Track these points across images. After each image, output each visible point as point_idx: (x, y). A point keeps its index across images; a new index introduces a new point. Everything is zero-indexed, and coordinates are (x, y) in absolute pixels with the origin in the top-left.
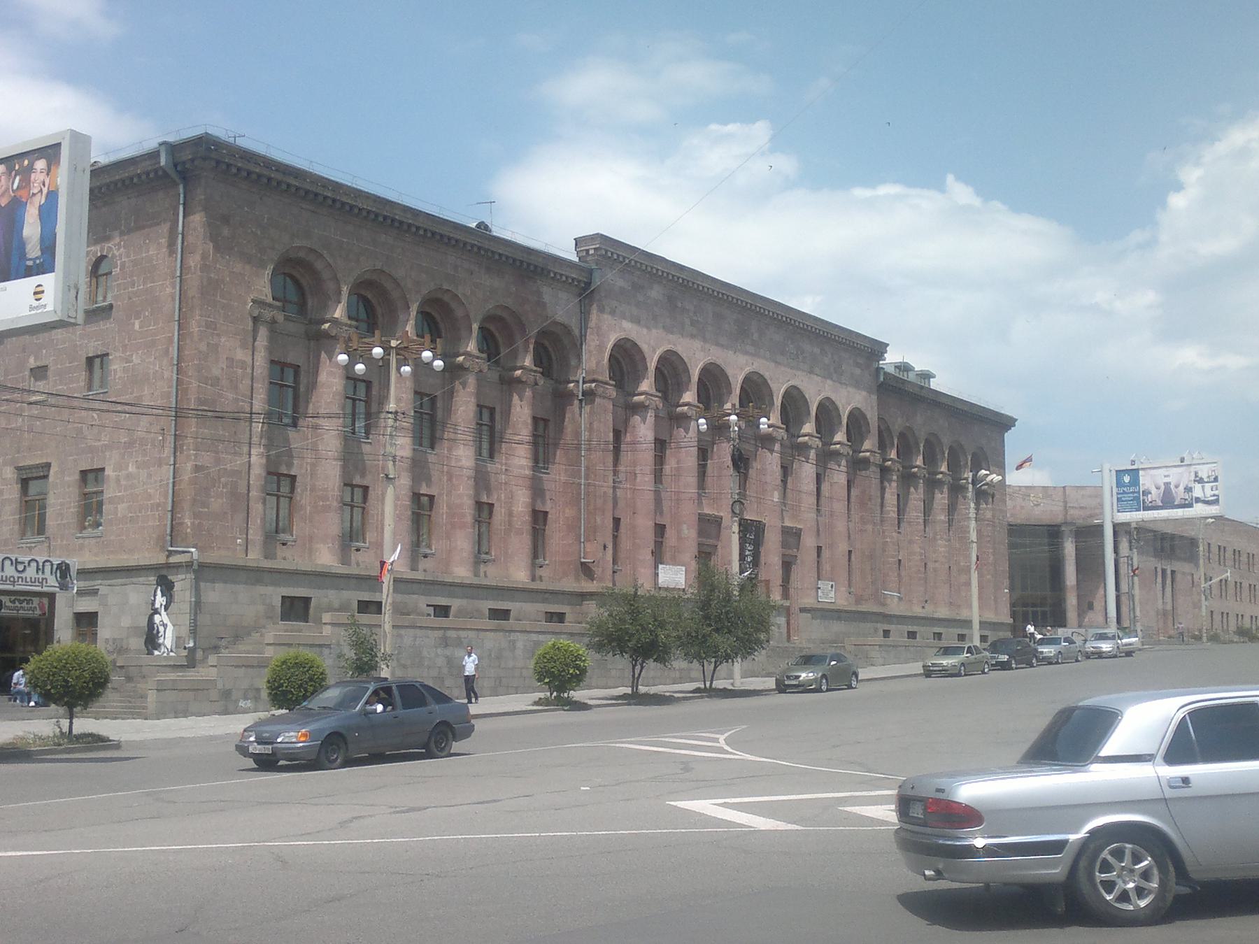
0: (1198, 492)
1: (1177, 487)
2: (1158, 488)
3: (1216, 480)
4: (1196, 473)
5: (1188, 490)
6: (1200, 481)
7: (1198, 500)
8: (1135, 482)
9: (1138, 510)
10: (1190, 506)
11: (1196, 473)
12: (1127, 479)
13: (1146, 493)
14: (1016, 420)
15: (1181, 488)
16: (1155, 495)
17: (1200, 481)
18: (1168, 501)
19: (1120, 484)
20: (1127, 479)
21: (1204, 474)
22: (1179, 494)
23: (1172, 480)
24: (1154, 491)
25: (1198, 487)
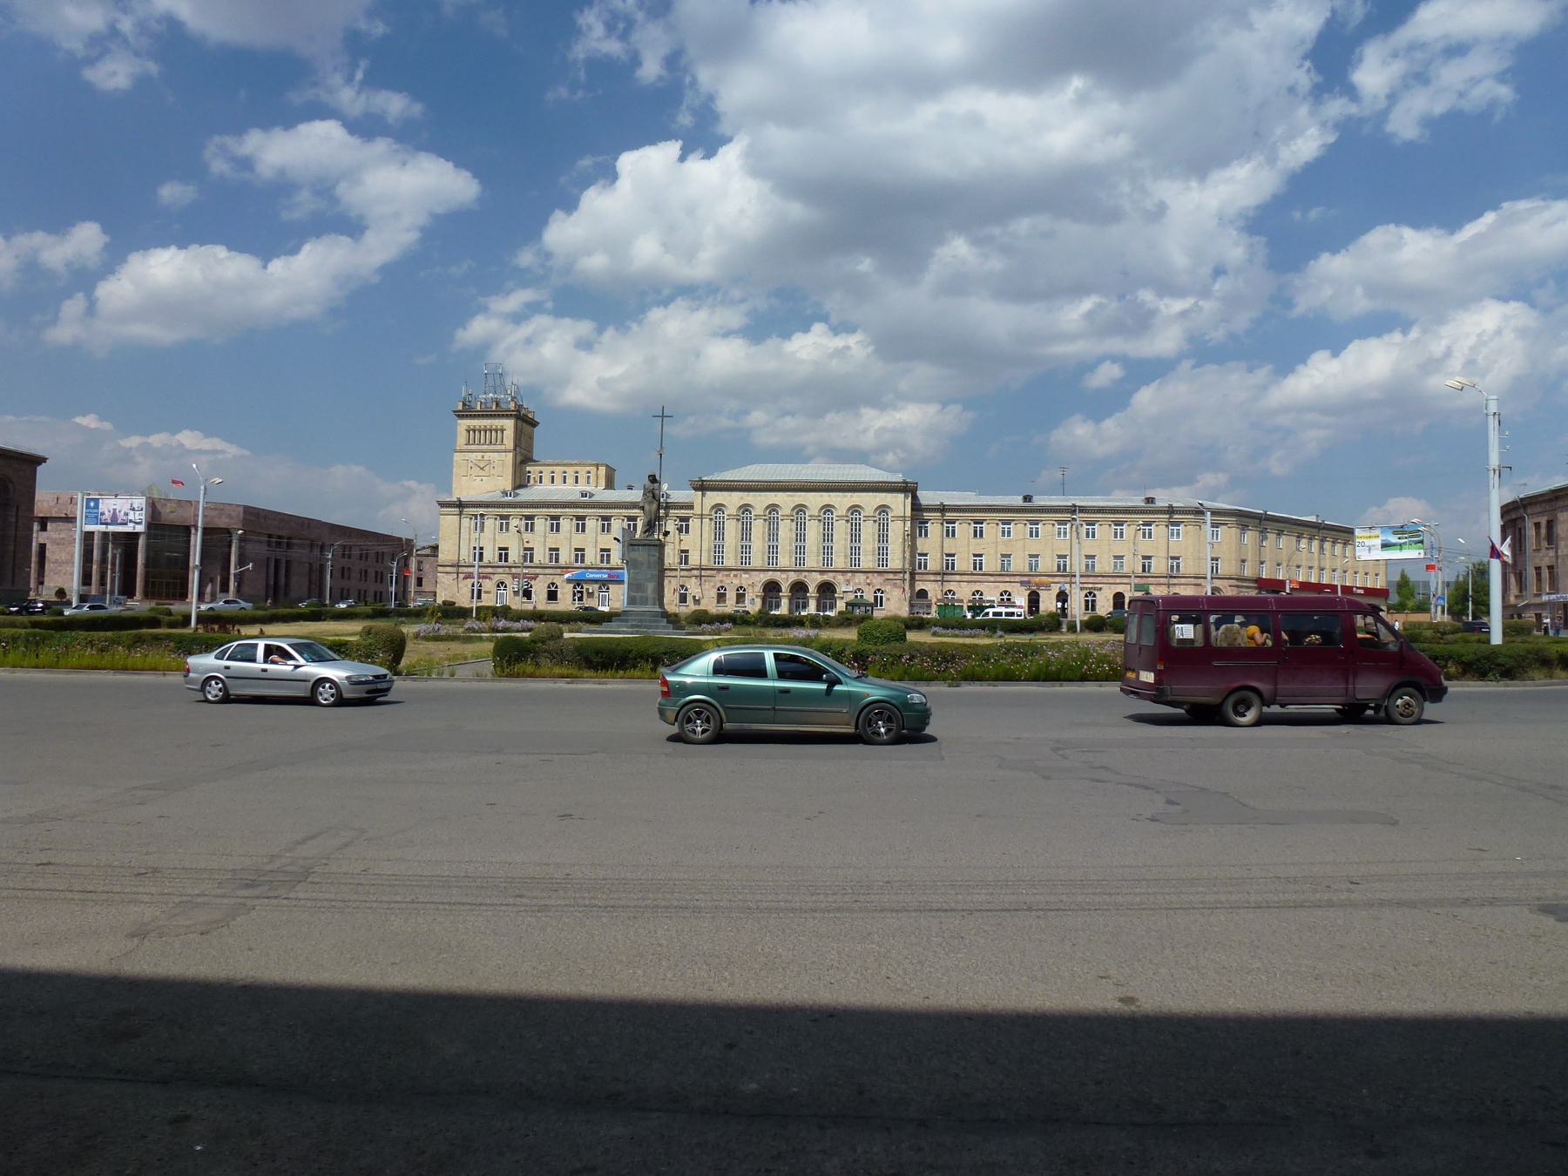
0: (131, 517)
1: (120, 512)
2: (109, 511)
3: (142, 510)
4: (132, 505)
5: (127, 514)
6: (133, 509)
7: (131, 521)
8: (97, 506)
9: (97, 524)
10: (126, 524)
11: (132, 505)
12: (92, 504)
13: (103, 514)
14: (47, 459)
15: (122, 513)
16: (108, 516)
17: (133, 509)
18: (114, 521)
19: (87, 507)
20: (92, 504)
21: (135, 506)
22: (121, 517)
23: (118, 508)
24: (107, 513)
25: (132, 512)
